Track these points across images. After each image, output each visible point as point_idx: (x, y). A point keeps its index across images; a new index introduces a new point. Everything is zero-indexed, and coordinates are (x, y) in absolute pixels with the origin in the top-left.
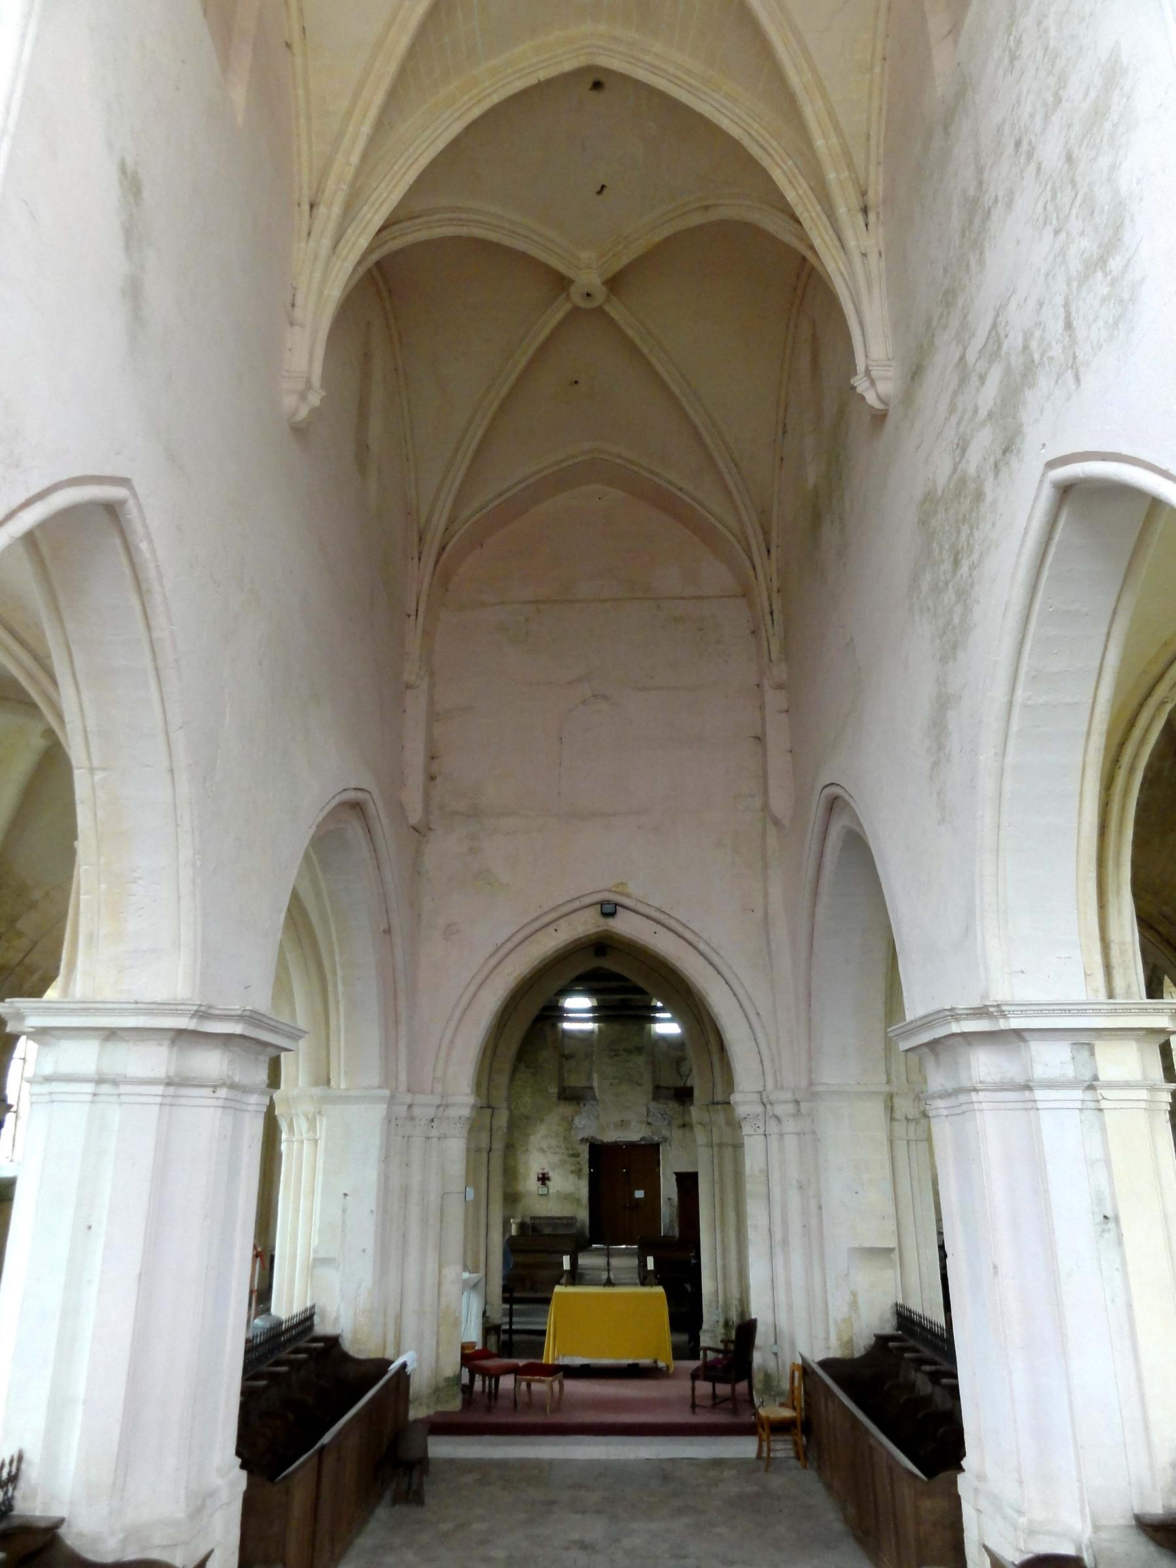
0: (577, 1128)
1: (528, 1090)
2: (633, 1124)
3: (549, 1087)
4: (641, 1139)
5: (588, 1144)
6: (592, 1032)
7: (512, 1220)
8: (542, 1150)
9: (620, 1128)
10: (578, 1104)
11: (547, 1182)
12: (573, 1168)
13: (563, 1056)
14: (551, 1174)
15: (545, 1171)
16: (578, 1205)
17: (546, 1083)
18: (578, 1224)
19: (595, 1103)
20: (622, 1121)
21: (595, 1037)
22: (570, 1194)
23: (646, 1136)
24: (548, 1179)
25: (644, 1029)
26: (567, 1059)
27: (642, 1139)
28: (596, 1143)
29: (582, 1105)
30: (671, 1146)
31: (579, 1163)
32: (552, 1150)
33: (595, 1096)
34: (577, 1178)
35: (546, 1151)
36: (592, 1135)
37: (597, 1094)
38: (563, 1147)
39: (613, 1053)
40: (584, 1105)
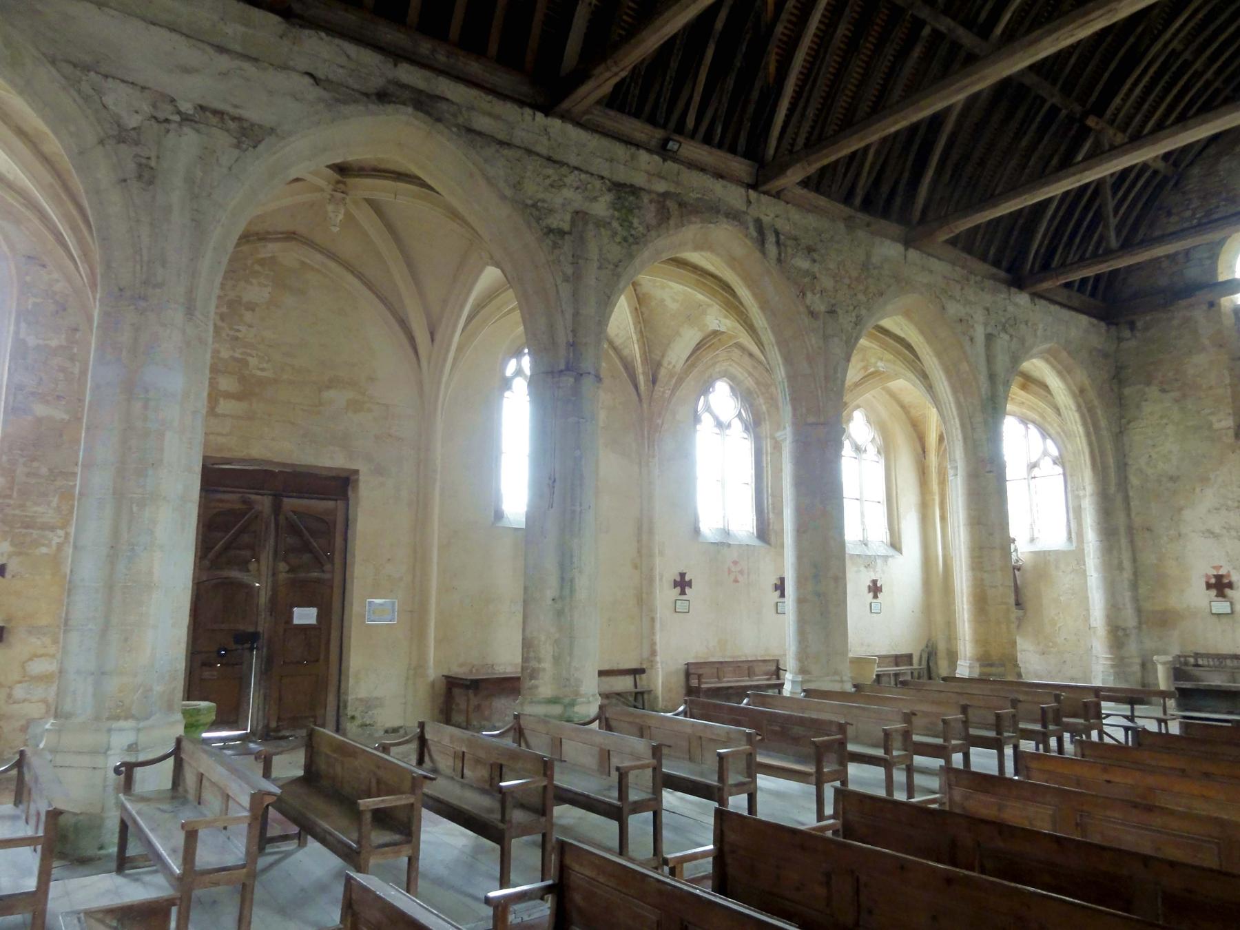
1: (1170, 429)
3: (1214, 419)
8: (1211, 533)
11: (1228, 592)
14: (1235, 578)
15: (1221, 572)
17: (1207, 411)
24: (1230, 585)
32: (1233, 533)
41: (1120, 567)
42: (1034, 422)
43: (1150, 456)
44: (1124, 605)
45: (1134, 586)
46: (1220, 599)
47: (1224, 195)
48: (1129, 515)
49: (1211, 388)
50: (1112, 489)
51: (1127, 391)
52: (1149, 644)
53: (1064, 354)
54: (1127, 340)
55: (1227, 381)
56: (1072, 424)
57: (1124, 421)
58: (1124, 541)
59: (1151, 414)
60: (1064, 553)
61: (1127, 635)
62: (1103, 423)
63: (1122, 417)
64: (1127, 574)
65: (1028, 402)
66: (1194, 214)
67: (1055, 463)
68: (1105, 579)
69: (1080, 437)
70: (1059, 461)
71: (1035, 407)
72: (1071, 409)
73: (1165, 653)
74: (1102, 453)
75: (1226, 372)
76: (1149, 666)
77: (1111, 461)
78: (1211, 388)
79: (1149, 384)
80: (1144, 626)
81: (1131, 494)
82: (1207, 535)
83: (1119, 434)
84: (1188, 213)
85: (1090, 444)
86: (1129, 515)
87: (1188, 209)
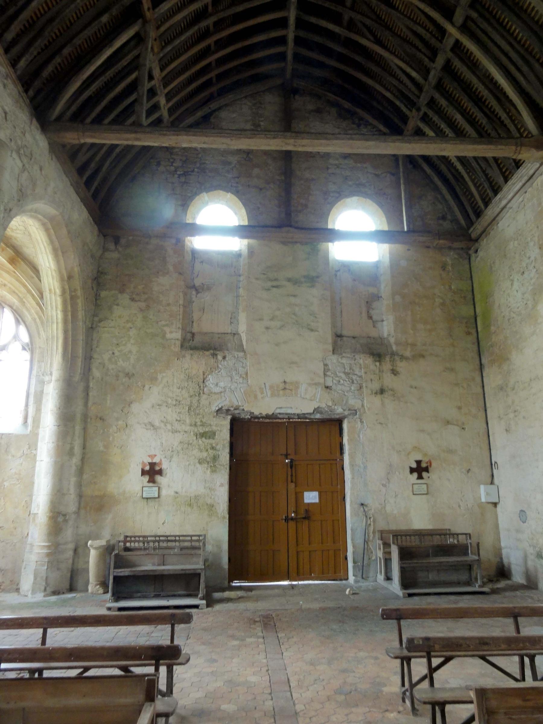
0: (210, 393)
1: (133, 332)
2: (303, 388)
3: (167, 329)
4: (315, 410)
5: (229, 417)
6: (239, 255)
7: (90, 543)
8: (152, 426)
9: (281, 392)
10: (214, 355)
11: (158, 478)
12: (205, 454)
13: (194, 287)
14: (164, 466)
15: (156, 460)
16: (210, 516)
17: (163, 323)
18: (209, 548)
19: (241, 354)
20: (285, 382)
21: (243, 261)
22: (197, 497)
23: (323, 405)
24: (160, 472)
25: (318, 251)
26: (198, 292)
27: (317, 410)
28: (243, 416)
29: (220, 358)
30: (362, 422)
31: (213, 448)
32: (169, 427)
33: (242, 345)
34: (208, 472)
35: (159, 428)
36: (236, 403)
37: (244, 343)
38: (188, 421)
39: (270, 284)
40: (224, 358)
41: (71, 453)
42: (11, 307)
43: (113, 353)
44: (69, 490)
45: (80, 471)
46: (151, 484)
47: (198, 165)
48: (86, 404)
49: (169, 305)
50: (77, 378)
51: (103, 294)
52: (84, 529)
53: (64, 231)
54: (111, 251)
55: (181, 302)
56: (52, 308)
57: (96, 319)
58: (78, 429)
59: (120, 317)
60: (18, 437)
61: (66, 521)
62: (81, 314)
63: (95, 315)
64: (76, 460)
65: (9, 285)
66: (176, 171)
67: (24, 349)
68: (56, 463)
69: (57, 323)
70: (30, 347)
71: (17, 291)
72: (55, 293)
73: (97, 537)
74: (74, 341)
75: (181, 295)
76: (80, 550)
77: (80, 352)
78: (169, 305)
79: (122, 291)
80: (82, 512)
81: (91, 385)
82: (148, 427)
83: (91, 329)
84: (172, 168)
85: (65, 332)
86: (86, 404)
87: (172, 165)
